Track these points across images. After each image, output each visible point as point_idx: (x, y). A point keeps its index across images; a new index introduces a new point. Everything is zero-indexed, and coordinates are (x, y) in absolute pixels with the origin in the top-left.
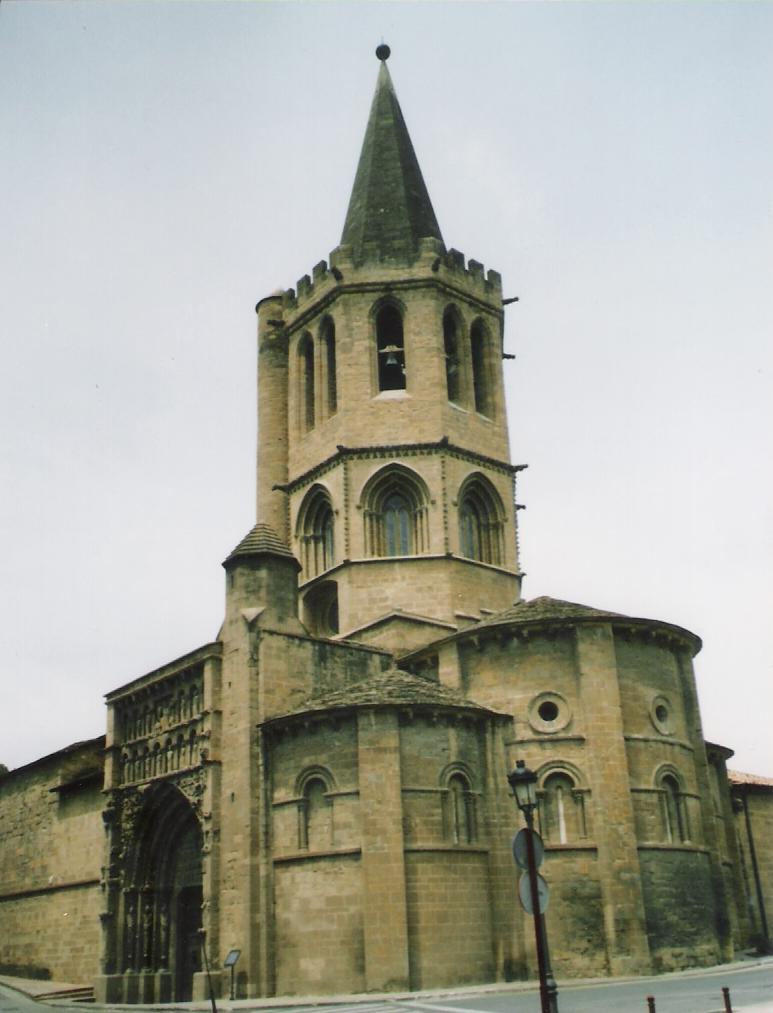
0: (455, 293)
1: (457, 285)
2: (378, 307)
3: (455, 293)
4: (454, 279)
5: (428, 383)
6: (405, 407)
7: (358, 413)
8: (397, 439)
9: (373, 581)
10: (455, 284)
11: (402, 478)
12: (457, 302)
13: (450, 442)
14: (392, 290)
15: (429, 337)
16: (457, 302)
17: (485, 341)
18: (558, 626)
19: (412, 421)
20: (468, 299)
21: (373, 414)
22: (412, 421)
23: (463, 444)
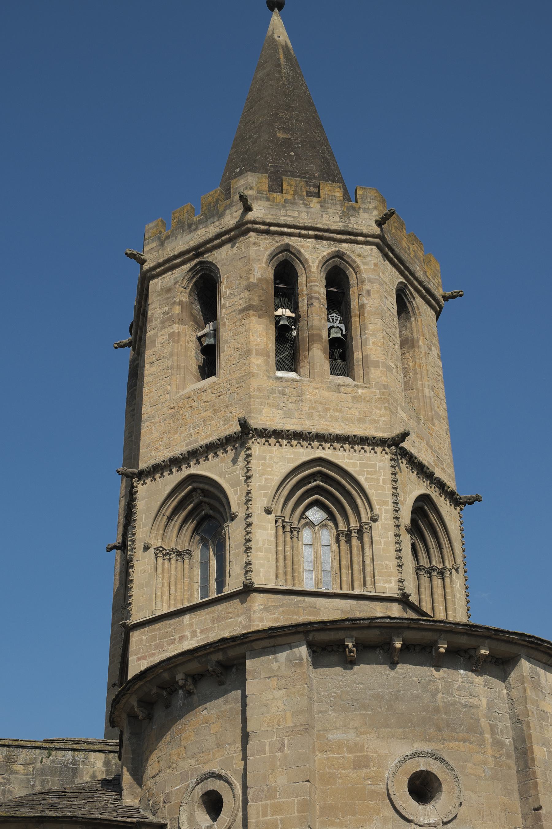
0: (286, 230)
1: (290, 220)
2: (189, 281)
3: (286, 230)
4: (283, 212)
5: (238, 353)
6: (210, 396)
7: (157, 419)
8: (196, 441)
9: (156, 647)
10: (282, 220)
11: (205, 493)
12: (293, 241)
13: (255, 423)
14: (202, 254)
15: (242, 295)
16: (293, 241)
17: (353, 279)
18: (219, 656)
19: (215, 412)
20: (311, 233)
21: (172, 415)
22: (215, 412)
23: (292, 426)
